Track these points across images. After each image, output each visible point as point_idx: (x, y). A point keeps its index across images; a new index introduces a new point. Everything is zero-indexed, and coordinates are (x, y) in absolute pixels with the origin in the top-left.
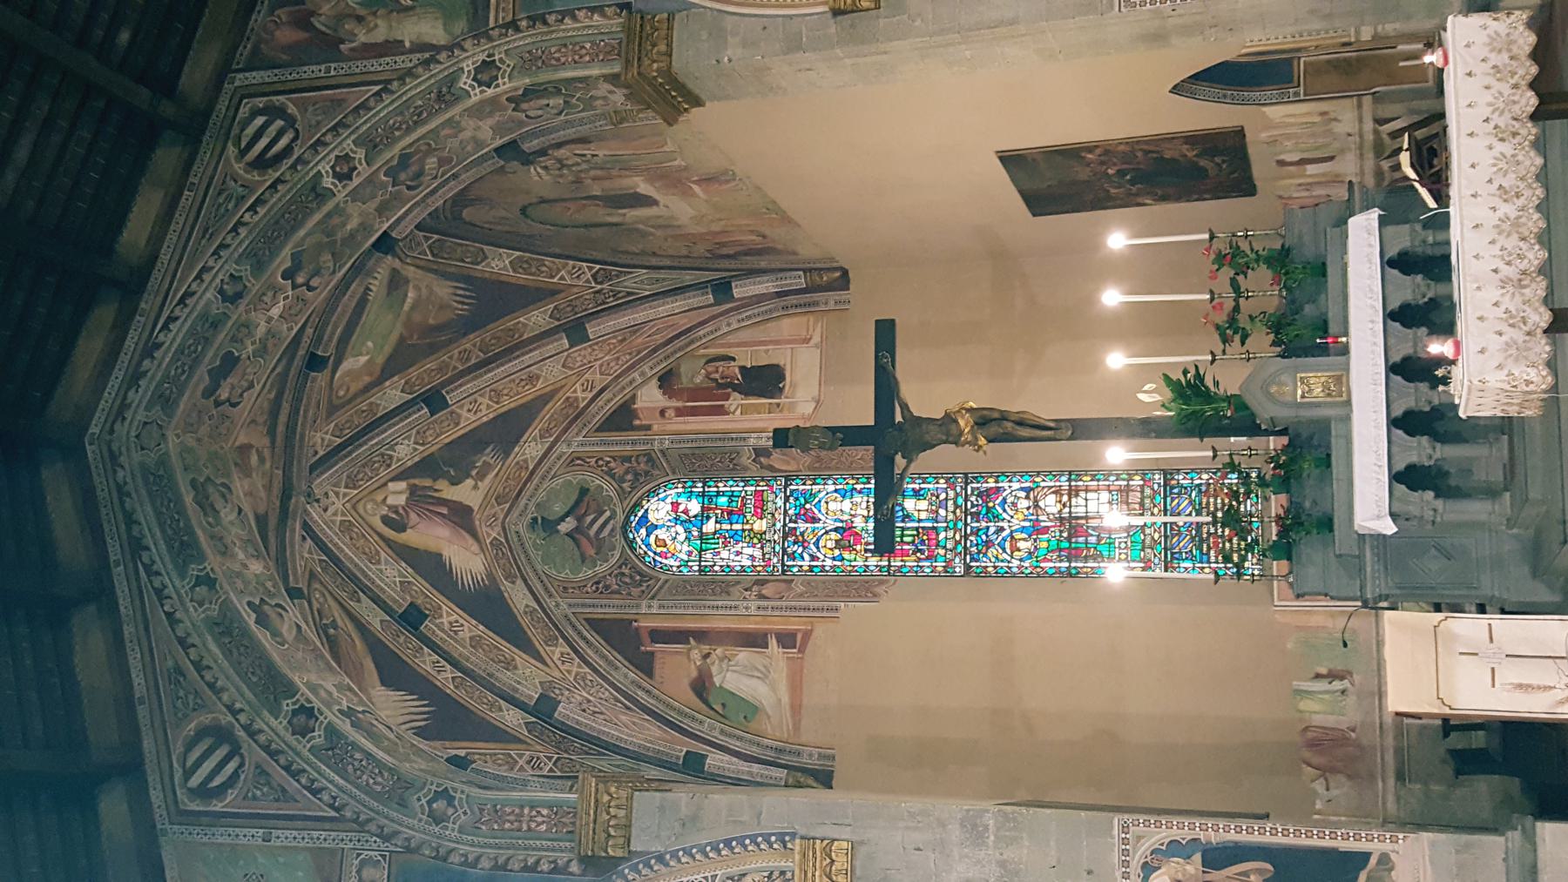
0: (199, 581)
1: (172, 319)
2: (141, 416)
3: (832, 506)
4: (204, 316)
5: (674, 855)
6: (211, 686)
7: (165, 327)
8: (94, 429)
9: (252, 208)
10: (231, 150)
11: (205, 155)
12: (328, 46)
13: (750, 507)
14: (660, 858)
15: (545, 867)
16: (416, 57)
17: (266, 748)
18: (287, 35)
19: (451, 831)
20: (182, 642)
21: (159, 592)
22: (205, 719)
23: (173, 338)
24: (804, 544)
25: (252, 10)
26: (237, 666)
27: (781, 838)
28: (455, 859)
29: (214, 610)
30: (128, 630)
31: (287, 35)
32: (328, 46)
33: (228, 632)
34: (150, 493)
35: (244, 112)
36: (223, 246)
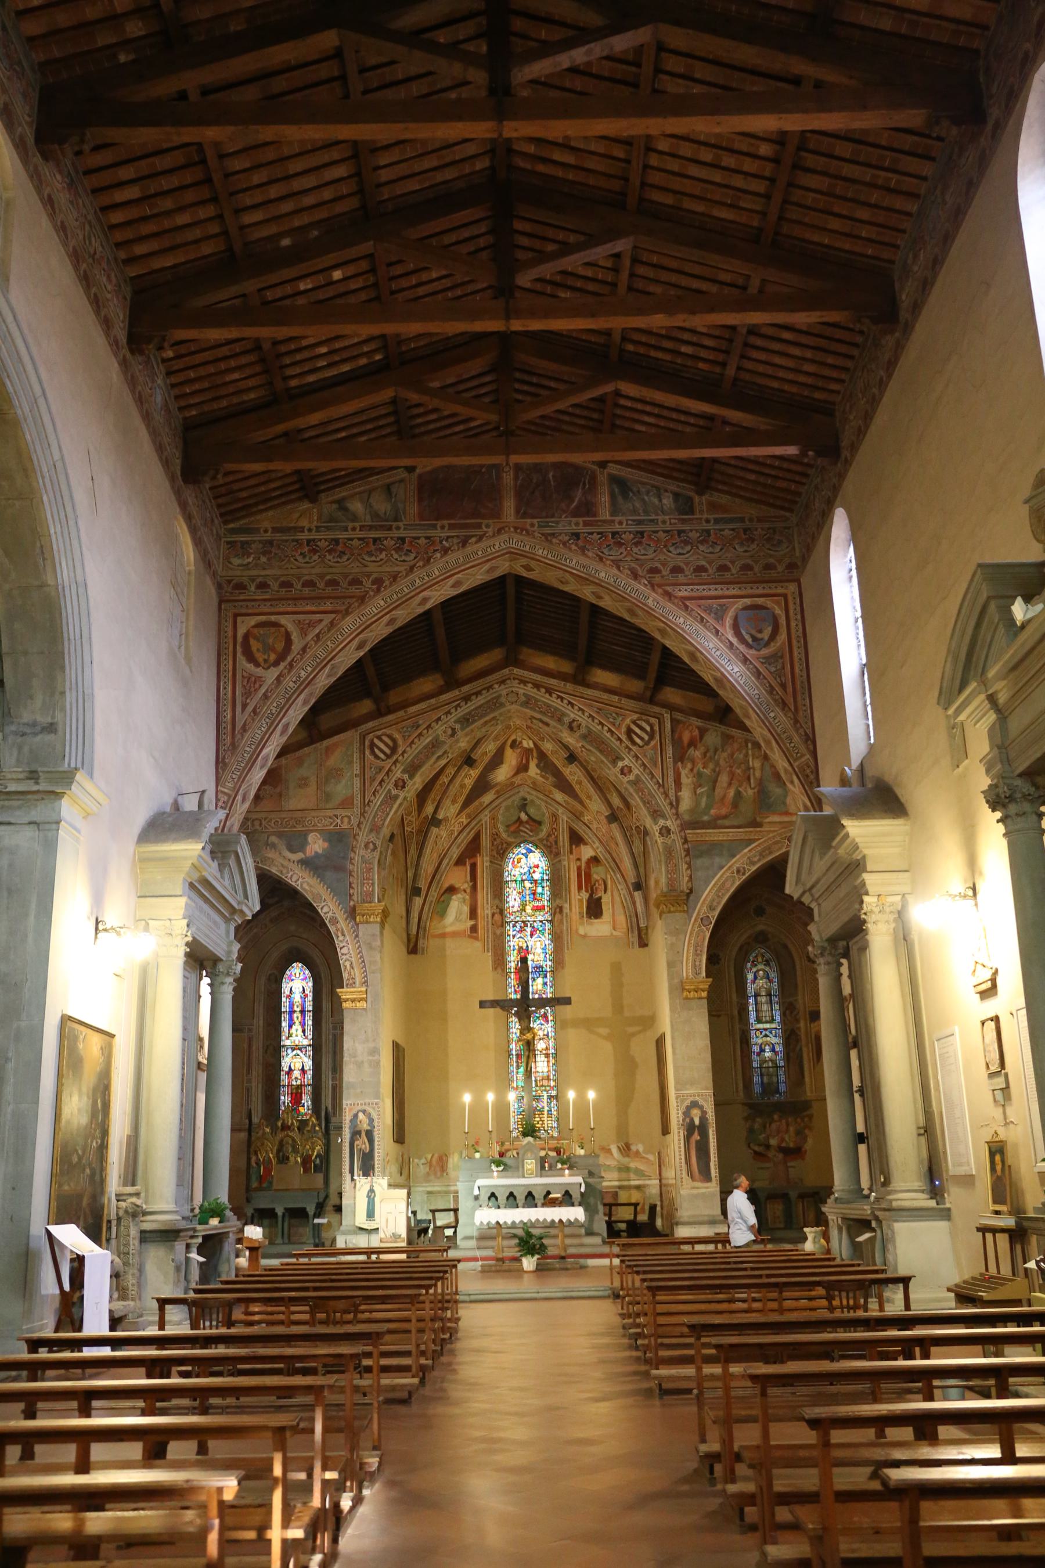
0: (453, 729)
1: (562, 699)
2: (521, 691)
3: (538, 944)
4: (564, 714)
5: (358, 941)
6: (412, 742)
7: (559, 697)
8: (516, 671)
9: (610, 730)
10: (635, 716)
11: (632, 704)
12: (680, 757)
13: (537, 904)
14: (357, 936)
15: (352, 891)
16: (673, 799)
17: (390, 770)
18: (686, 737)
19: (362, 852)
20: (429, 727)
21: (449, 713)
22: (400, 742)
23: (554, 701)
24: (521, 931)
25: (698, 717)
26: (420, 752)
27: (366, 982)
28: (352, 855)
29: (442, 738)
30: (433, 701)
31: (686, 737)
32: (680, 757)
33: (433, 746)
34: (489, 701)
35: (653, 720)
36: (593, 718)
